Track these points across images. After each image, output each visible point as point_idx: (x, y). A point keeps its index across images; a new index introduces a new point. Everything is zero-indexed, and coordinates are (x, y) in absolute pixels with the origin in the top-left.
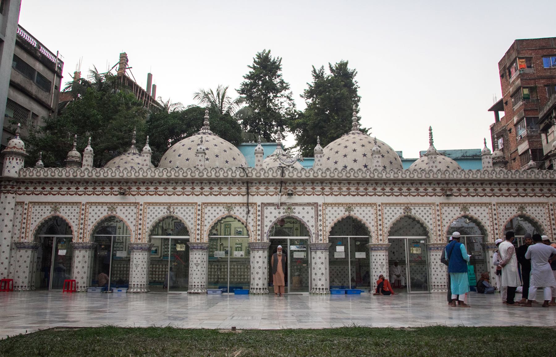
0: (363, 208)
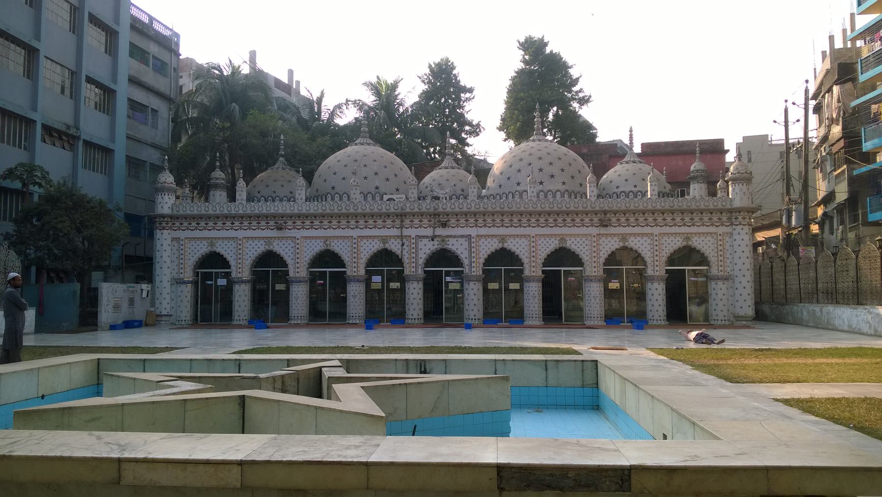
0: (518, 240)
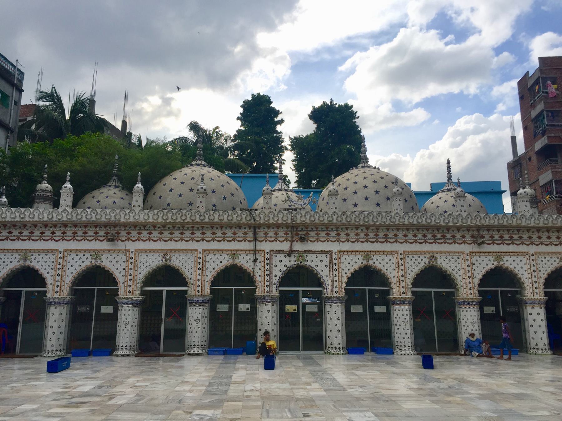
0: (383, 257)
